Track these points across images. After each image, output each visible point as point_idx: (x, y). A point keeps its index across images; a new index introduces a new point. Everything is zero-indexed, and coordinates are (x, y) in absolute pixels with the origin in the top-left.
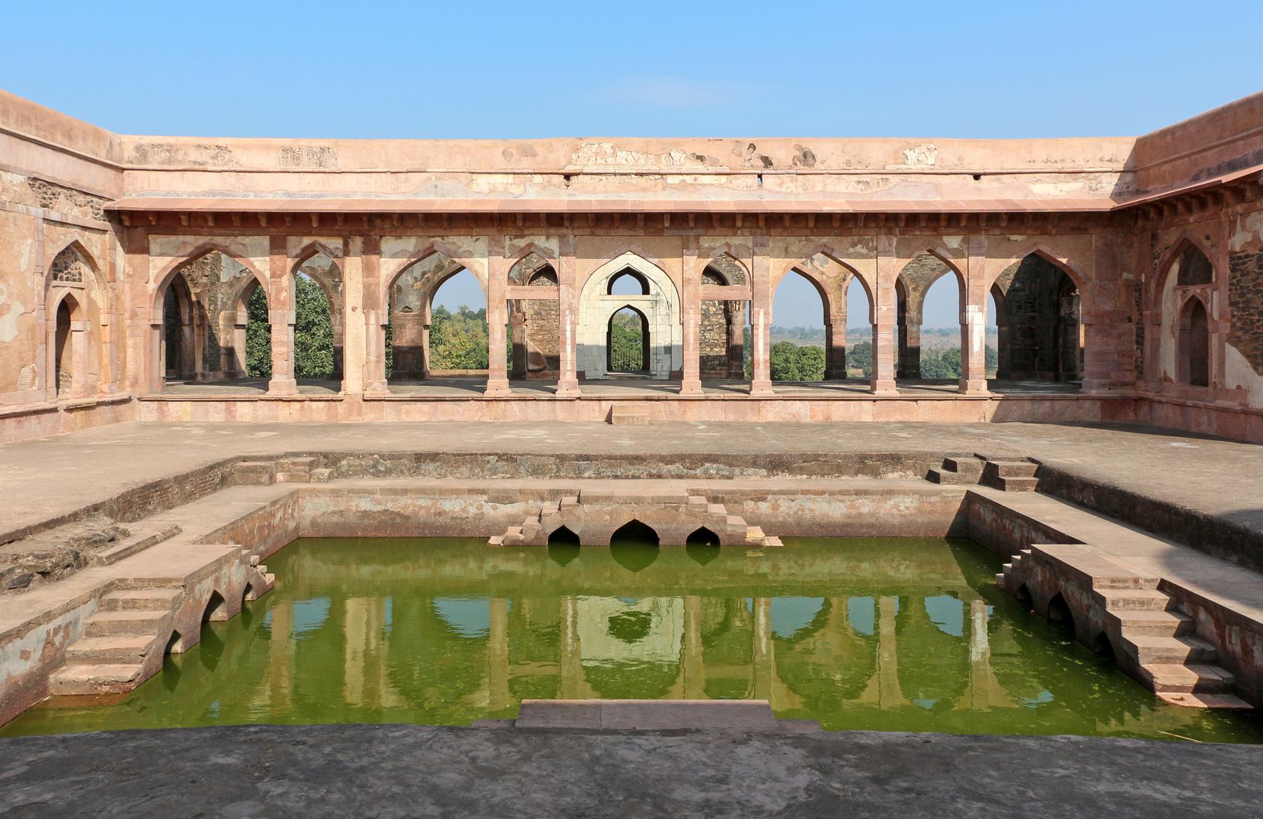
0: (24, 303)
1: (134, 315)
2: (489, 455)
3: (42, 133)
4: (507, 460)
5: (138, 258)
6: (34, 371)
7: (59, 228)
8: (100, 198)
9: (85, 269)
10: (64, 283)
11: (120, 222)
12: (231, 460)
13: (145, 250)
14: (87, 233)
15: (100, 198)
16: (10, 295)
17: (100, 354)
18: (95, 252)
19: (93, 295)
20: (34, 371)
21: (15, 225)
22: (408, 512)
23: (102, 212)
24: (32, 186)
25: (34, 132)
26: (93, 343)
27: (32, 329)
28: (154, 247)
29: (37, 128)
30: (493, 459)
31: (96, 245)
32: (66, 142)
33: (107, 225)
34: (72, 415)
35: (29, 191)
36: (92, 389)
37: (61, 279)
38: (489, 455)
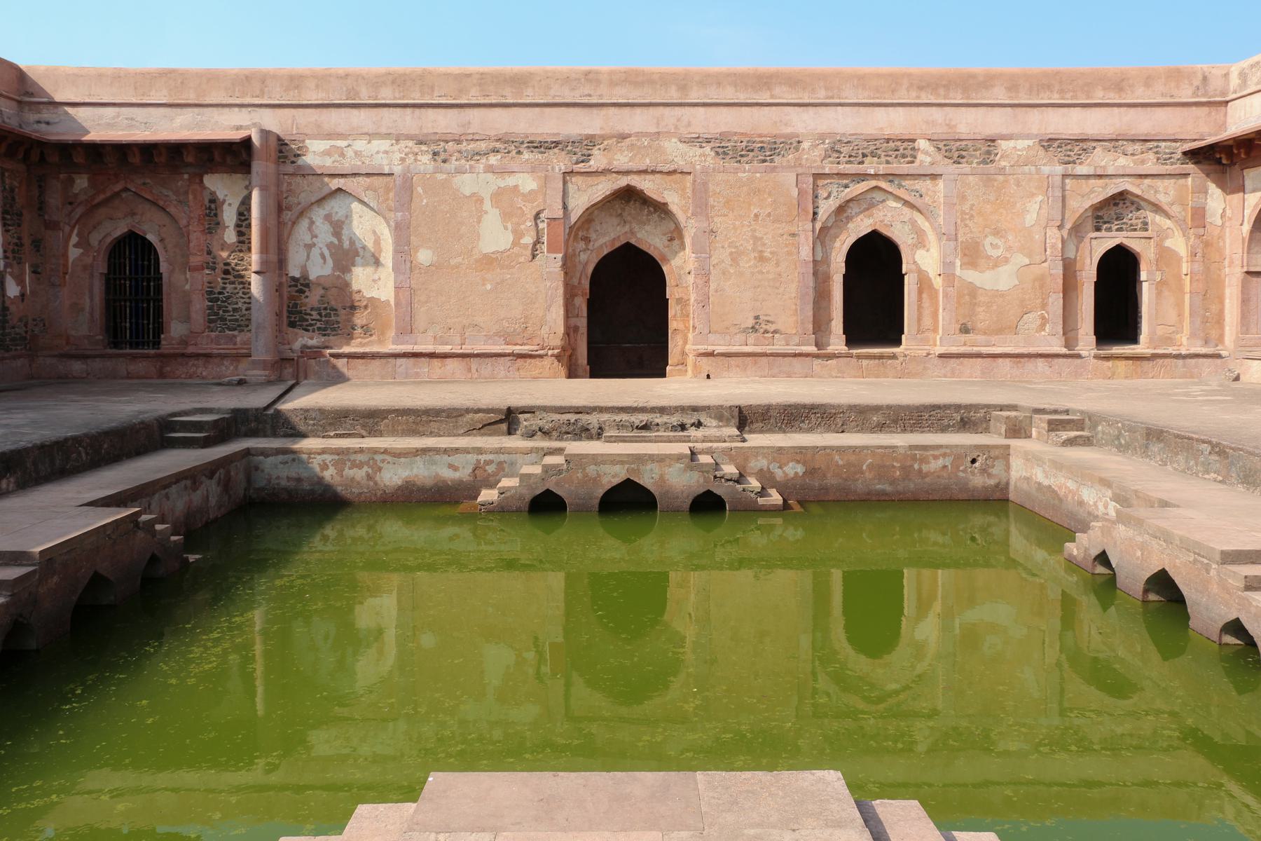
0: (1029, 256)
1: (1231, 263)
2: (1204, 442)
3: (1068, 95)
4: (1219, 453)
5: (1237, 197)
6: (1043, 318)
7: (1092, 181)
8: (1175, 141)
9: (1151, 217)
10: (1114, 233)
11: (1219, 162)
12: (988, 406)
13: (1242, 189)
14: (1147, 181)
15: (1175, 141)
16: (1009, 249)
17: (1179, 305)
18: (1163, 199)
19: (1168, 243)
20: (1043, 318)
21: (1018, 185)
22: (1062, 493)
23: (1179, 155)
24: (1046, 148)
25: (1056, 96)
26: (1166, 293)
27: (1041, 280)
28: (1248, 184)
29: (1061, 91)
30: (1206, 448)
31: (1164, 192)
32: (1112, 95)
33: (1190, 167)
34: (1110, 364)
35: (1042, 153)
36: (1168, 340)
37: (1109, 230)
38: (1204, 442)
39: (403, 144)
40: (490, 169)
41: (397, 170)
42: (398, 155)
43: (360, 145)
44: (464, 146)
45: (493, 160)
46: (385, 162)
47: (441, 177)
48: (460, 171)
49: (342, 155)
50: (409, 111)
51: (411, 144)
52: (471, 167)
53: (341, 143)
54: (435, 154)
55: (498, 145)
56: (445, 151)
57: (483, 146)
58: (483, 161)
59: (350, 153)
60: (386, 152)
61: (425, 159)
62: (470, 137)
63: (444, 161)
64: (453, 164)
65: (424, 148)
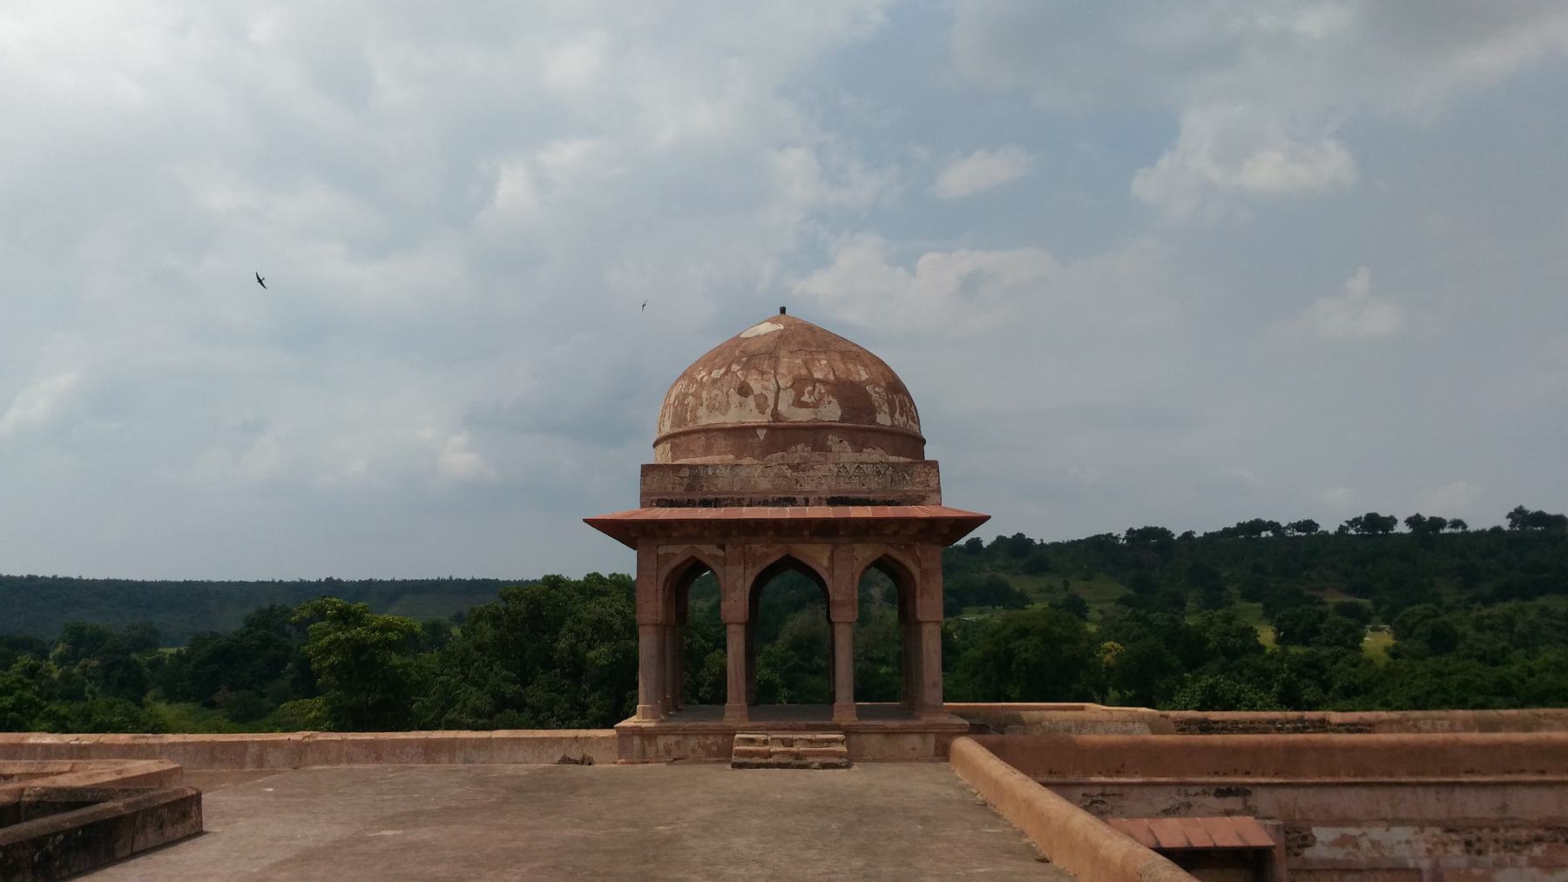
39: (1429, 831)
40: (1534, 862)
41: (1425, 864)
42: (1423, 846)
43: (1377, 833)
44: (1502, 834)
45: (1538, 850)
46: (1407, 854)
47: (1476, 872)
48: (1500, 865)
49: (1357, 846)
50: (1432, 790)
51: (1438, 831)
52: (1512, 859)
53: (1352, 831)
54: (1468, 844)
55: (1540, 832)
56: (1479, 840)
57: (1523, 834)
58: (1526, 852)
59: (1365, 844)
60: (1408, 842)
61: (1456, 850)
62: (1507, 823)
63: (1479, 853)
64: (1491, 857)
65: (1453, 836)
